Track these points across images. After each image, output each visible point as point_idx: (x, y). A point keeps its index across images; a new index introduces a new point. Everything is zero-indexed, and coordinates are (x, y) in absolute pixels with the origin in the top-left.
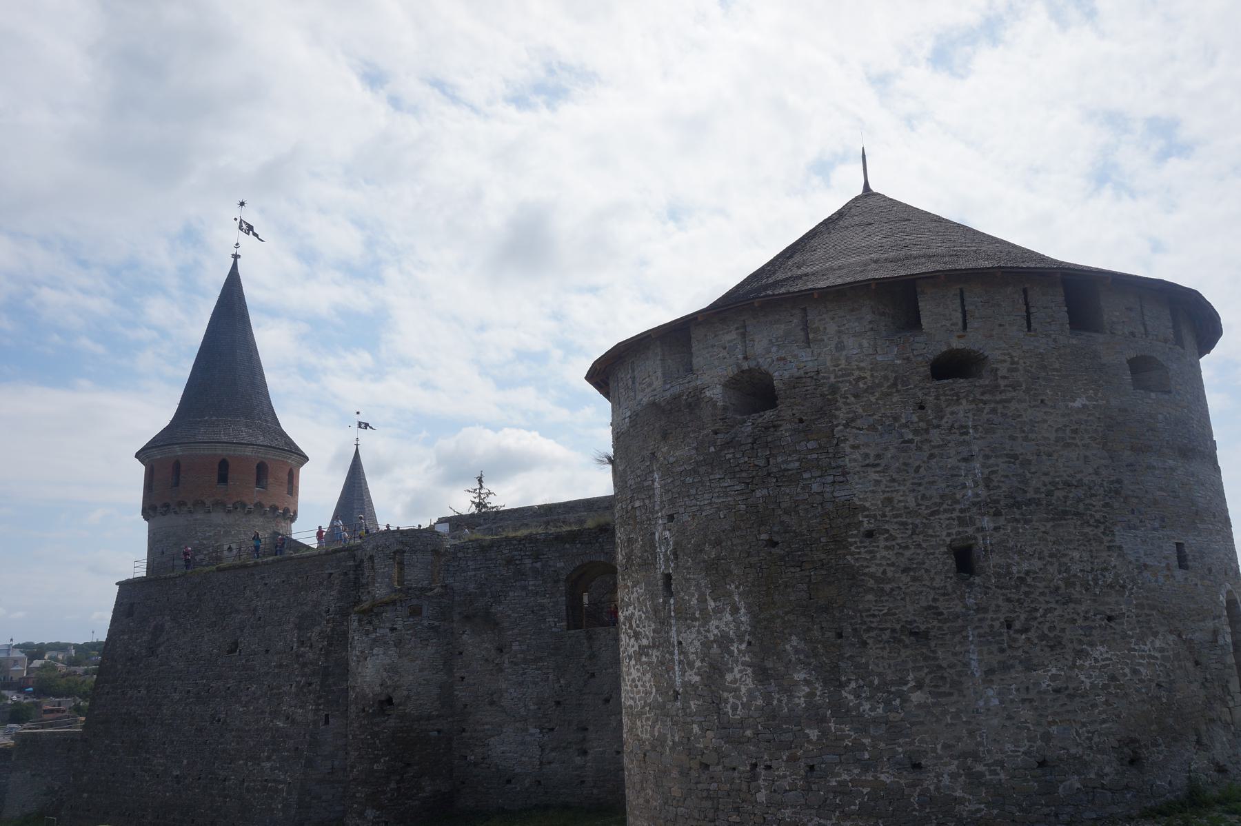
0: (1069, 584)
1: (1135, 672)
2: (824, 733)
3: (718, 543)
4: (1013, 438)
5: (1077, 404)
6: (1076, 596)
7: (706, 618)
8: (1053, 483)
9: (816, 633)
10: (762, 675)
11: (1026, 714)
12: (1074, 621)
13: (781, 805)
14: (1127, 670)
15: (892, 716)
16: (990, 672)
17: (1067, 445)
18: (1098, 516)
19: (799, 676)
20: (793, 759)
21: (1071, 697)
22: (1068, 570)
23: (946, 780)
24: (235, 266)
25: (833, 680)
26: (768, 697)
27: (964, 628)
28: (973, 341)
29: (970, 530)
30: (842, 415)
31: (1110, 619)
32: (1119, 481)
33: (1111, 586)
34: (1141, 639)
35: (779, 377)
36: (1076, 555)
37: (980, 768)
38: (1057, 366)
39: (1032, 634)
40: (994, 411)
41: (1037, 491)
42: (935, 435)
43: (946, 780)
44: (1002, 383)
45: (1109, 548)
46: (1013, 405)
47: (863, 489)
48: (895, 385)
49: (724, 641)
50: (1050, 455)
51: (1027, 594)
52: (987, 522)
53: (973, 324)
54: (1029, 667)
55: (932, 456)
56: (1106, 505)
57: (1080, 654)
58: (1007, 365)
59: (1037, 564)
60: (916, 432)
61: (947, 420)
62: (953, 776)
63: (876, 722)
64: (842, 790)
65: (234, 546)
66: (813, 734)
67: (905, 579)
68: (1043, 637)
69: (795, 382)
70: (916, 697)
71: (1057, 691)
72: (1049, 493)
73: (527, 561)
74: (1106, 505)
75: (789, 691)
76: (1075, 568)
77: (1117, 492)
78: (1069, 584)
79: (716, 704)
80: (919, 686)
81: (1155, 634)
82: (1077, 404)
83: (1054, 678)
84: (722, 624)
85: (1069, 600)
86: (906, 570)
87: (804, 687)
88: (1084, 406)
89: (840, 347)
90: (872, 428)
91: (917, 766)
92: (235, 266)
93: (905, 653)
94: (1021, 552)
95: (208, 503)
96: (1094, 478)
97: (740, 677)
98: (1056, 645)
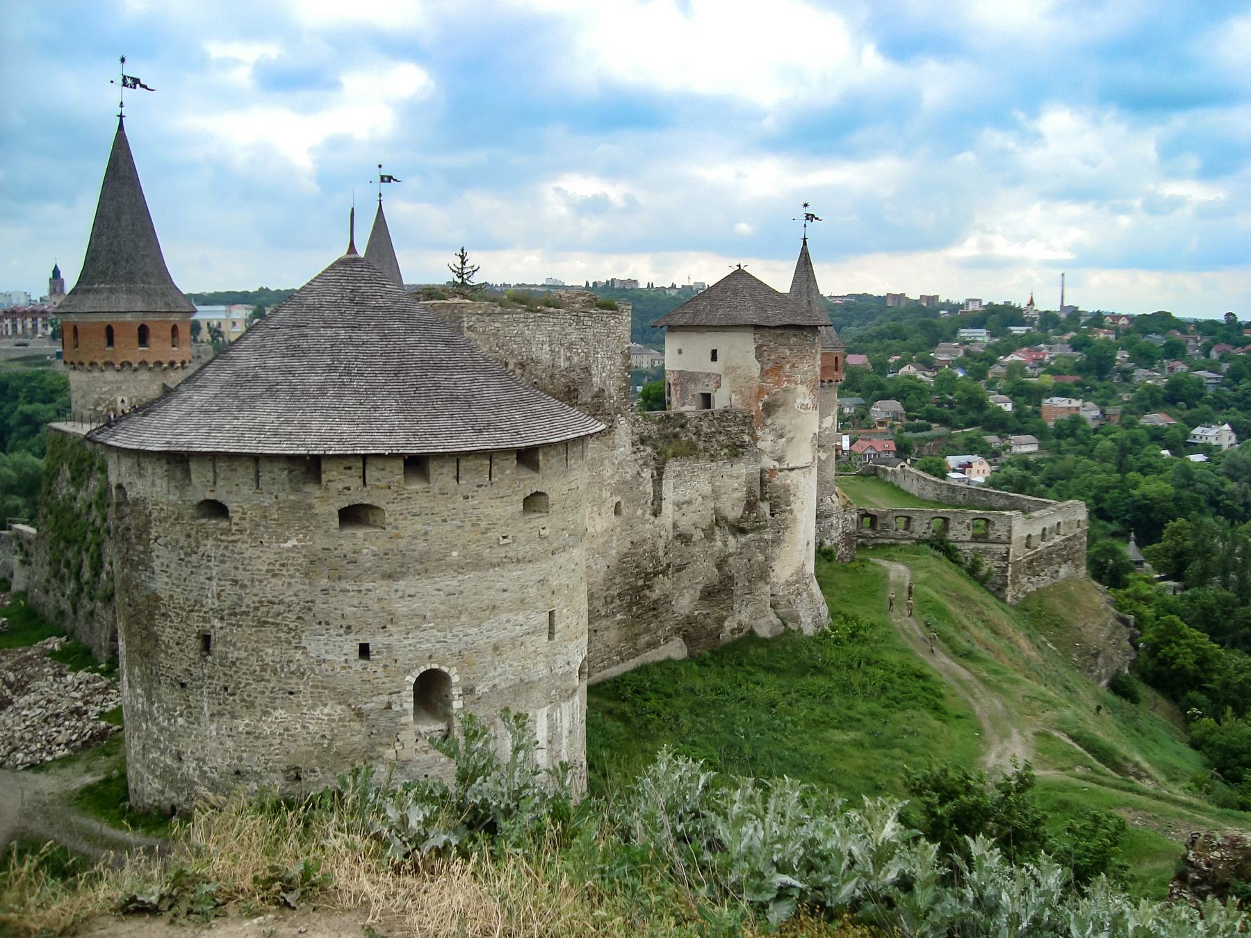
0: (263, 669)
1: (304, 727)
4: (236, 568)
5: (289, 544)
6: (267, 677)
8: (261, 602)
11: (229, 743)
12: (263, 693)
14: (298, 726)
16: (212, 715)
17: (274, 576)
18: (291, 625)
21: (257, 738)
22: (263, 660)
23: (191, 771)
24: (121, 127)
27: (201, 687)
28: (221, 495)
29: (208, 626)
31: (291, 693)
32: (312, 601)
33: (293, 673)
34: (313, 707)
36: (270, 651)
37: (206, 768)
38: (275, 516)
39: (237, 697)
40: (226, 548)
41: (248, 606)
42: (194, 558)
43: (191, 771)
44: (234, 528)
45: (296, 648)
46: (239, 544)
47: (160, 584)
48: (177, 519)
50: (261, 581)
51: (236, 672)
52: (217, 623)
53: (220, 483)
54: (233, 716)
55: (192, 573)
56: (299, 618)
57: (266, 713)
58: (240, 514)
59: (243, 654)
60: (186, 554)
61: (202, 549)
62: (194, 769)
65: (126, 399)
67: (177, 649)
68: (243, 700)
70: (180, 721)
71: (248, 733)
72: (257, 609)
74: (299, 618)
76: (268, 660)
77: (310, 609)
78: (263, 669)
80: (181, 715)
81: (325, 705)
82: (289, 544)
83: (247, 725)
86: (178, 644)
88: (295, 546)
89: (153, 485)
90: (165, 545)
92: (121, 127)
93: (176, 694)
94: (234, 645)
95: (100, 362)
96: (294, 598)
98: (250, 706)
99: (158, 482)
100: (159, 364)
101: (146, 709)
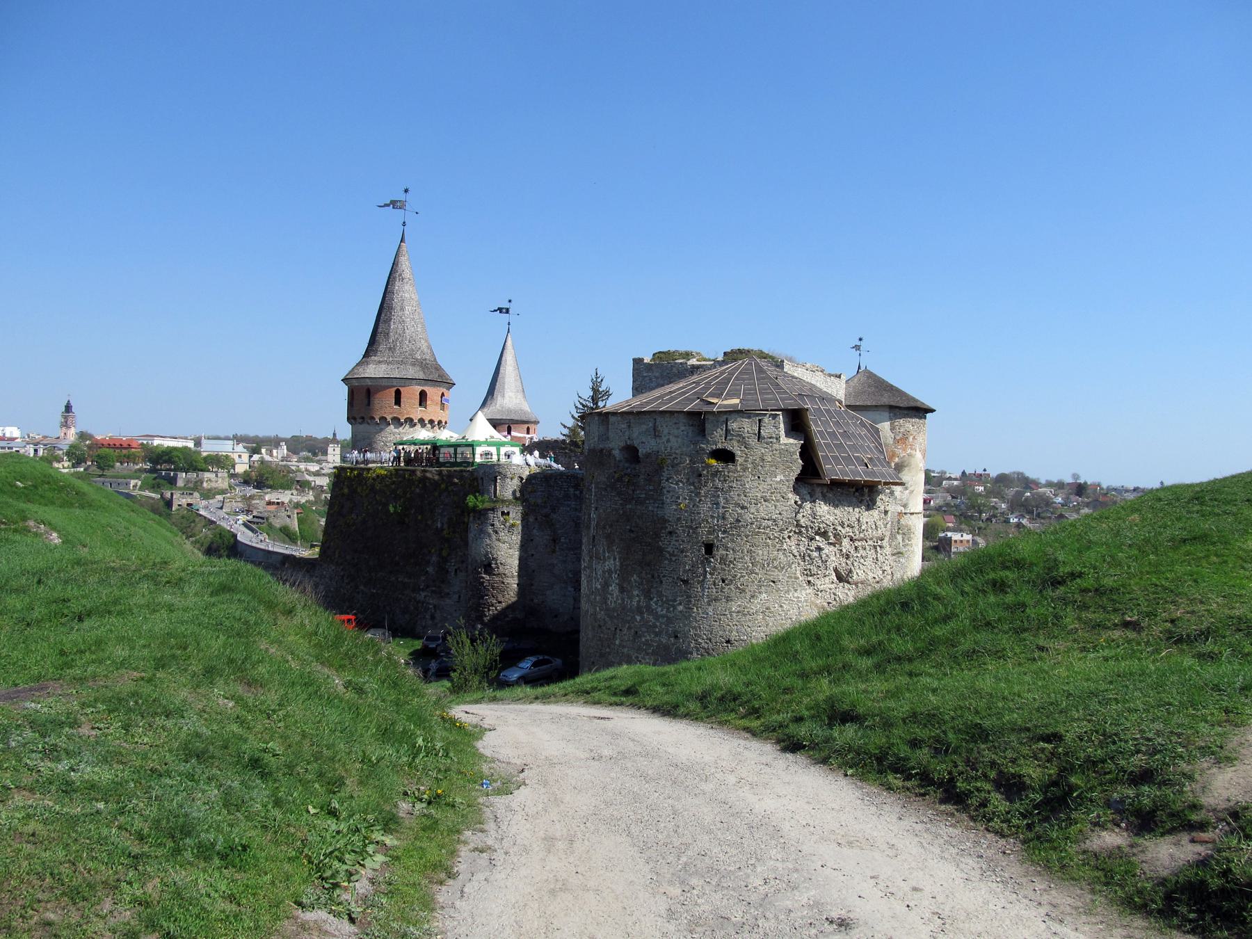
2: (643, 618)
3: (611, 526)
7: (605, 560)
9: (643, 575)
10: (622, 590)
13: (624, 647)
15: (671, 615)
19: (636, 593)
20: (630, 628)
25: (647, 595)
26: (623, 599)
30: (665, 474)
34: (788, 592)
35: (642, 451)
39: (732, 587)
49: (610, 571)
63: (663, 616)
64: (647, 643)
66: (638, 618)
69: (648, 455)
73: (572, 490)
75: (631, 598)
79: (605, 600)
82: (778, 479)
84: (610, 564)
85: (752, 572)
87: (636, 598)
89: (668, 441)
91: (676, 637)
97: (614, 588)
99: (673, 439)
100: (431, 422)
101: (643, 604)
